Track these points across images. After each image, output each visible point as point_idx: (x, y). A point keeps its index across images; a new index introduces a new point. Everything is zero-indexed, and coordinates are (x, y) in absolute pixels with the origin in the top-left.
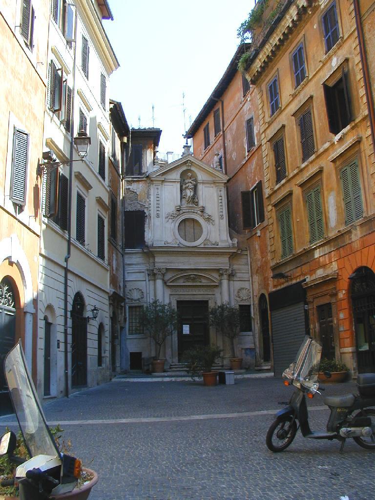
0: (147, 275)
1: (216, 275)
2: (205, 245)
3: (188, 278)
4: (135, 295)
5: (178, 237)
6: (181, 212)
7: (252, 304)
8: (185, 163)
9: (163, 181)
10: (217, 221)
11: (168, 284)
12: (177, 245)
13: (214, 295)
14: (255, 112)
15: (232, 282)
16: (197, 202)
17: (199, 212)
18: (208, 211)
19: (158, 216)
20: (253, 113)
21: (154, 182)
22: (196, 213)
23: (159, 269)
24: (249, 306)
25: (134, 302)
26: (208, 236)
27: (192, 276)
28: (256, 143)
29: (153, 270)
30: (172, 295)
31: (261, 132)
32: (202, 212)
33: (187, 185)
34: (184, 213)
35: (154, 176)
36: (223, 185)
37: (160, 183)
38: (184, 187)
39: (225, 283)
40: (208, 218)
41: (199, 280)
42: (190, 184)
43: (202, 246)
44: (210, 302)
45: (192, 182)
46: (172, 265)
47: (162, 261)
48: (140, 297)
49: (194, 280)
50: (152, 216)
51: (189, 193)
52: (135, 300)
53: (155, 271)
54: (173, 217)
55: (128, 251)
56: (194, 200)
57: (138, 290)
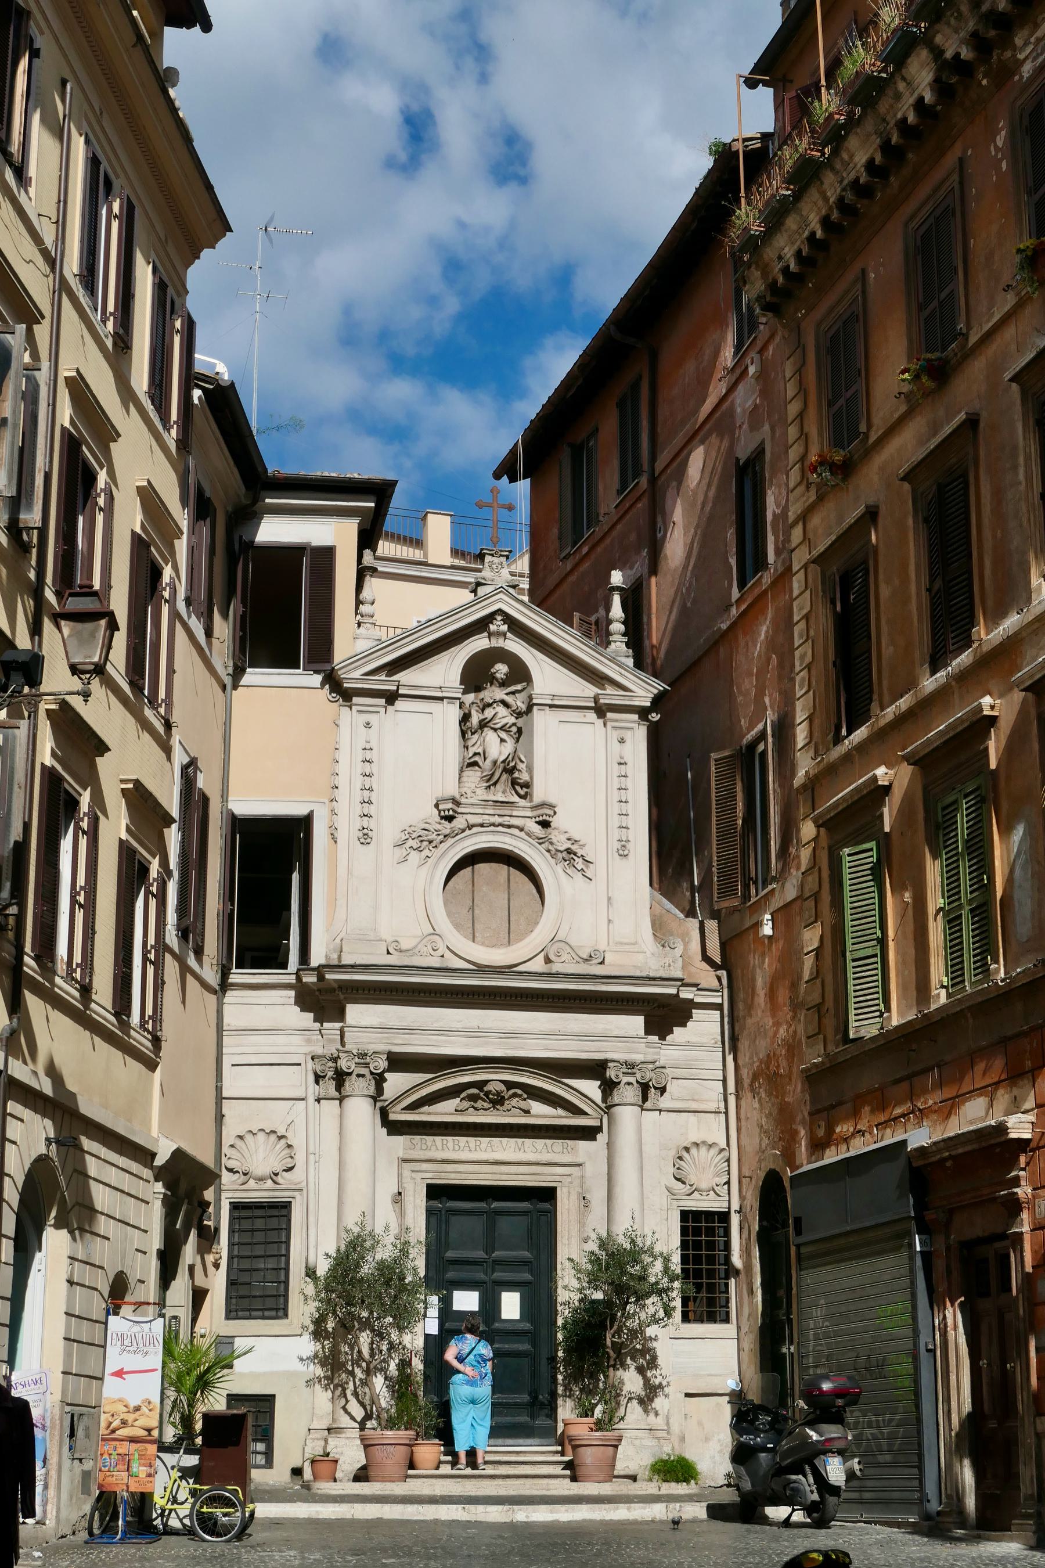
0: (311, 1078)
1: (591, 1088)
2: (548, 960)
3: (477, 1093)
4: (261, 1155)
5: (444, 924)
6: (459, 822)
8: (481, 626)
9: (391, 698)
10: (598, 871)
11: (392, 1117)
12: (435, 962)
13: (579, 1165)
14: (773, 429)
15: (650, 1117)
16: (527, 785)
18: (567, 823)
19: (365, 837)
20: (767, 427)
21: (355, 700)
23: (362, 1055)
24: (724, 1217)
25: (252, 1183)
26: (565, 928)
27: (489, 1087)
28: (771, 557)
29: (335, 1060)
30: (405, 1161)
31: (792, 516)
32: (545, 824)
33: (489, 713)
35: (357, 674)
36: (635, 717)
38: (475, 719)
39: (627, 1115)
40: (569, 851)
41: (523, 1104)
42: (502, 710)
43: (537, 965)
44: (560, 1194)
45: (509, 699)
46: (415, 1038)
47: (375, 1022)
48: (278, 1168)
49: (498, 1101)
50: (342, 836)
51: (496, 747)
52: (261, 1179)
53: (343, 1064)
54: (422, 841)
55: (237, 976)
56: (511, 776)
57: (273, 1137)
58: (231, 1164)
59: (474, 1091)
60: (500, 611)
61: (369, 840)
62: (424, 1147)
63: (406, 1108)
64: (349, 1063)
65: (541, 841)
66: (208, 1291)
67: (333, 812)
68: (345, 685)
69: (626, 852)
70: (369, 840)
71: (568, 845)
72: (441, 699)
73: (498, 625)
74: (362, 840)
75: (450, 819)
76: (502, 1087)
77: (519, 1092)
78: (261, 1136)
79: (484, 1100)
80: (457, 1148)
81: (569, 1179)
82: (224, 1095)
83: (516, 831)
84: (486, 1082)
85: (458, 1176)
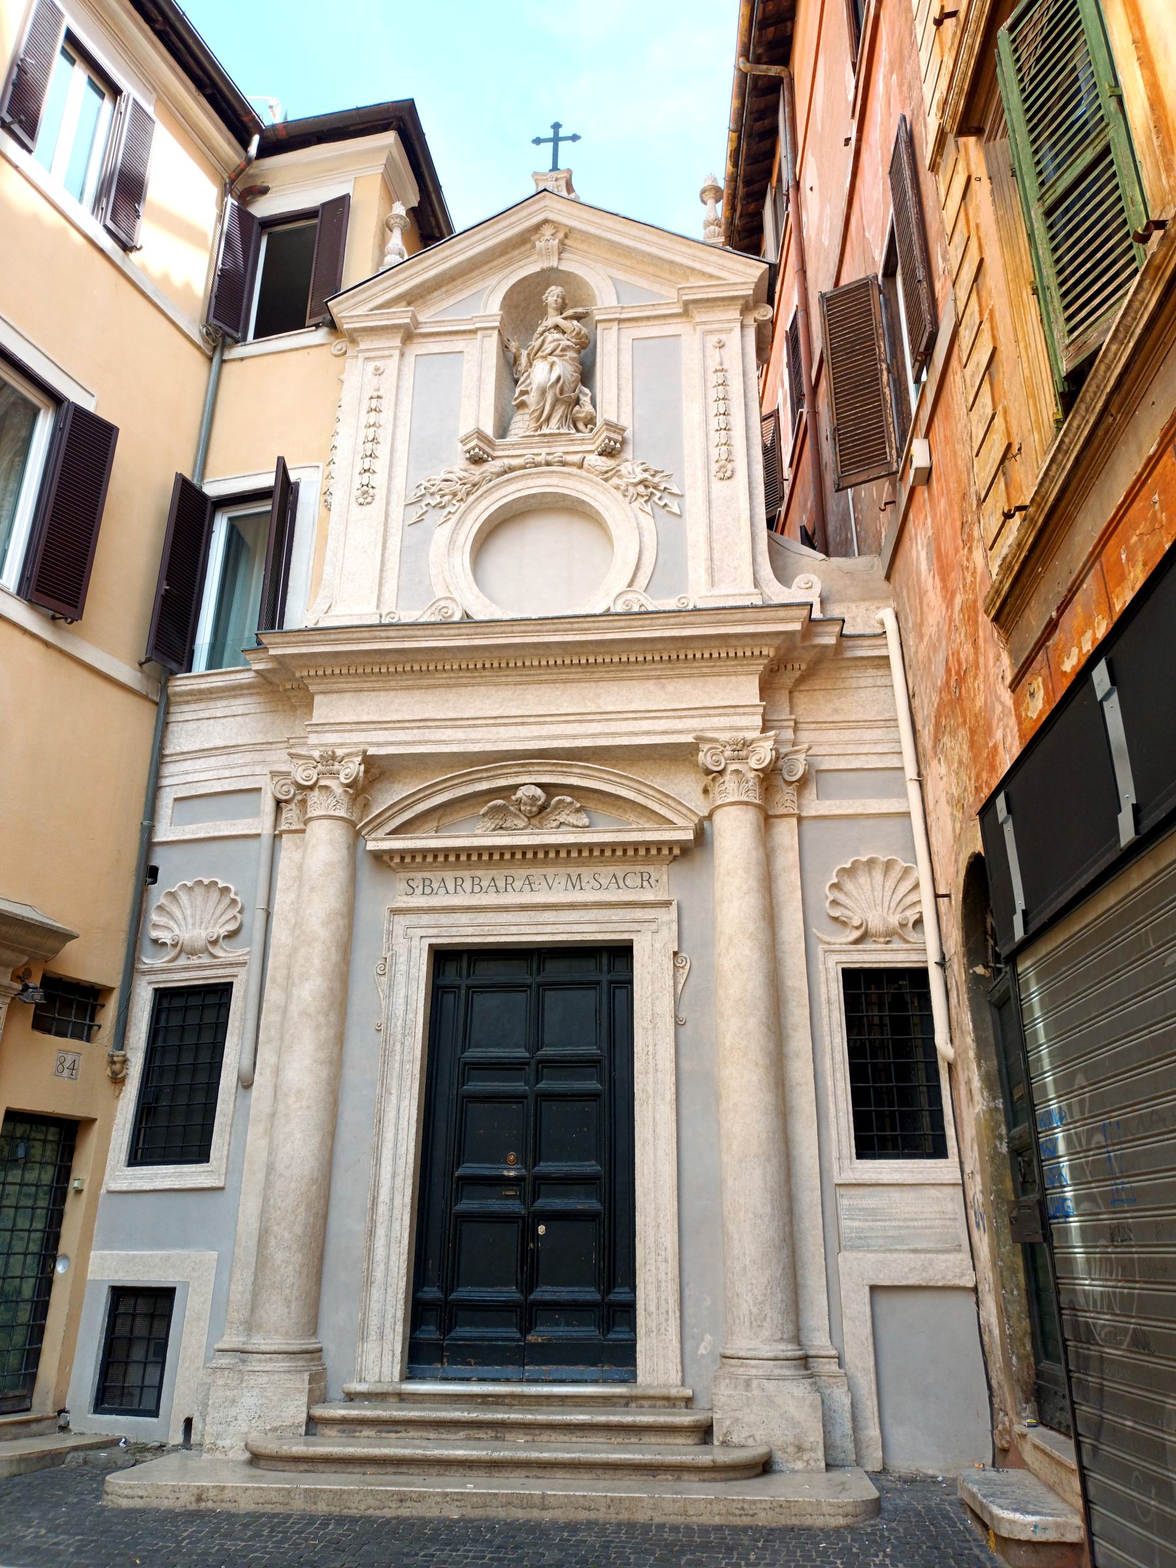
6: (492, 467)
7: (932, 957)
9: (409, 335)
17: (593, 460)
22: (580, 466)
34: (511, 469)
37: (397, 342)
58: (154, 934)
59: (500, 802)
60: (546, 221)
61: (369, 499)
62: (428, 890)
63: (394, 832)
64: (306, 773)
65: (606, 475)
66: (91, 1121)
67: (329, 477)
68: (345, 326)
69: (728, 474)
70: (369, 499)
71: (646, 475)
72: (474, 332)
73: (547, 240)
74: (361, 500)
75: (477, 460)
76: (539, 792)
77: (569, 799)
78: (199, 891)
79: (516, 816)
80: (477, 889)
81: (654, 926)
82: (156, 840)
83: (574, 470)
84: (516, 787)
85: (478, 930)
